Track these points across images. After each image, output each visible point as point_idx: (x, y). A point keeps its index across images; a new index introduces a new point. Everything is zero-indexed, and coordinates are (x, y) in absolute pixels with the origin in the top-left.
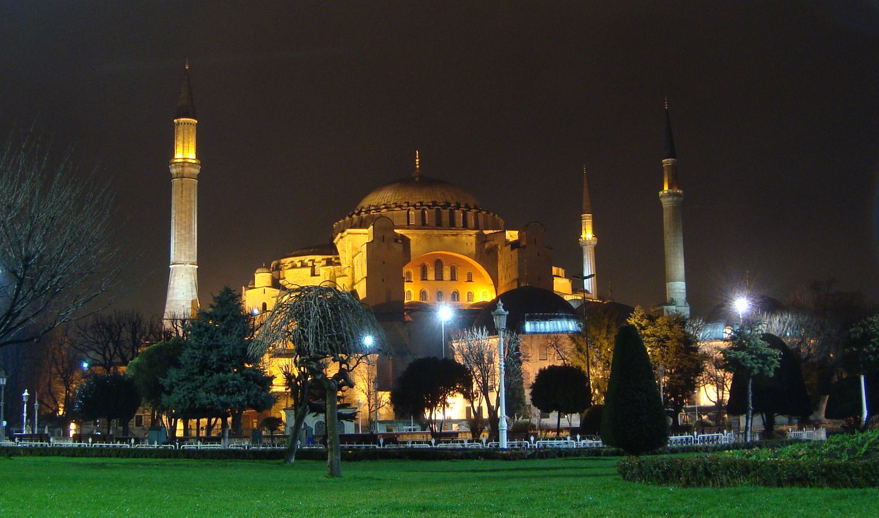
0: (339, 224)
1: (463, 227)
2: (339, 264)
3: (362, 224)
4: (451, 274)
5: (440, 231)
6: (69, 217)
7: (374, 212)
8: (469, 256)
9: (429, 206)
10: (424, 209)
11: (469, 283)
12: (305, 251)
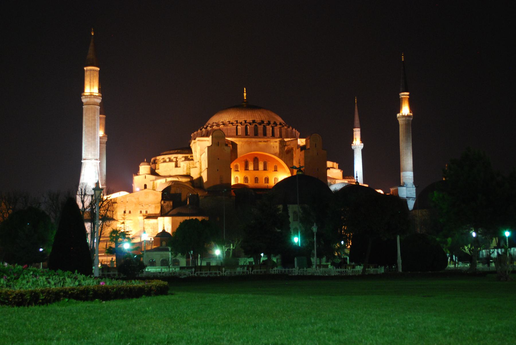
0: (194, 134)
1: (271, 136)
2: (192, 160)
3: (207, 135)
4: (264, 166)
5: (256, 139)
7: (216, 127)
8: (275, 154)
9: (250, 123)
10: (246, 126)
11: (275, 172)
12: (172, 152)
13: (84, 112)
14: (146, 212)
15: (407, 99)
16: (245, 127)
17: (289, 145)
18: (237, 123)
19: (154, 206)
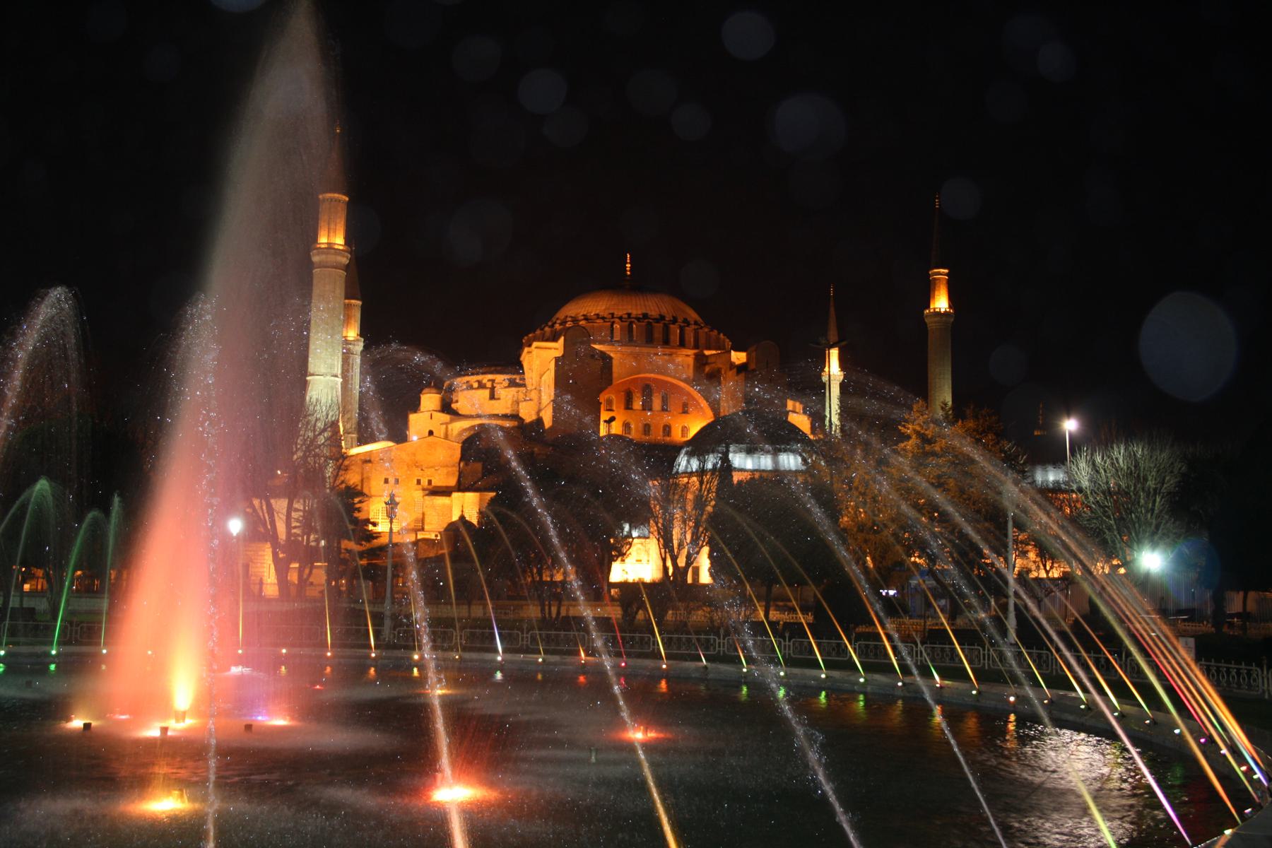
2: (524, 385)
3: (554, 338)
6: (211, 326)
8: (685, 381)
10: (631, 323)
11: (684, 415)
13: (315, 282)
14: (430, 482)
15: (945, 282)
16: (629, 325)
17: (714, 363)
18: (613, 317)
19: (445, 470)
